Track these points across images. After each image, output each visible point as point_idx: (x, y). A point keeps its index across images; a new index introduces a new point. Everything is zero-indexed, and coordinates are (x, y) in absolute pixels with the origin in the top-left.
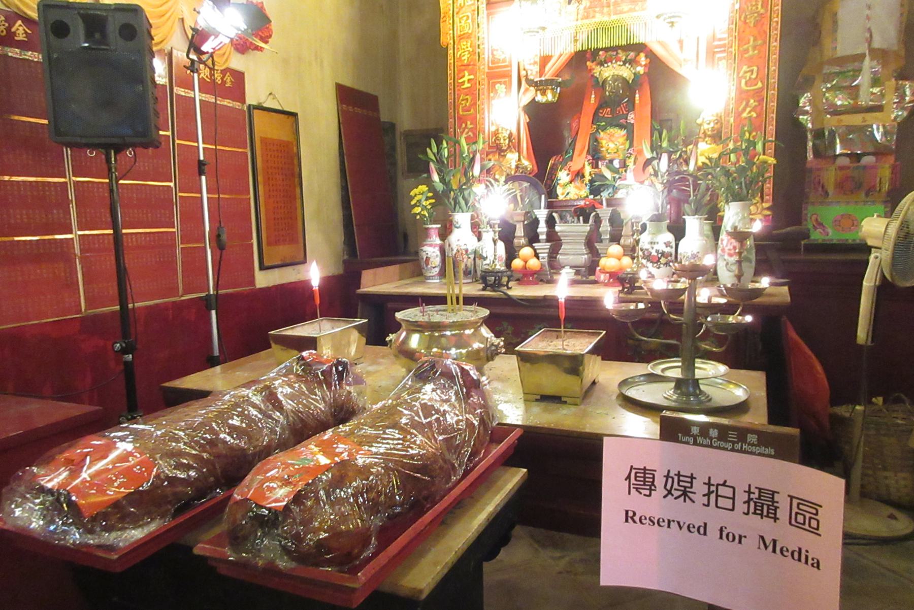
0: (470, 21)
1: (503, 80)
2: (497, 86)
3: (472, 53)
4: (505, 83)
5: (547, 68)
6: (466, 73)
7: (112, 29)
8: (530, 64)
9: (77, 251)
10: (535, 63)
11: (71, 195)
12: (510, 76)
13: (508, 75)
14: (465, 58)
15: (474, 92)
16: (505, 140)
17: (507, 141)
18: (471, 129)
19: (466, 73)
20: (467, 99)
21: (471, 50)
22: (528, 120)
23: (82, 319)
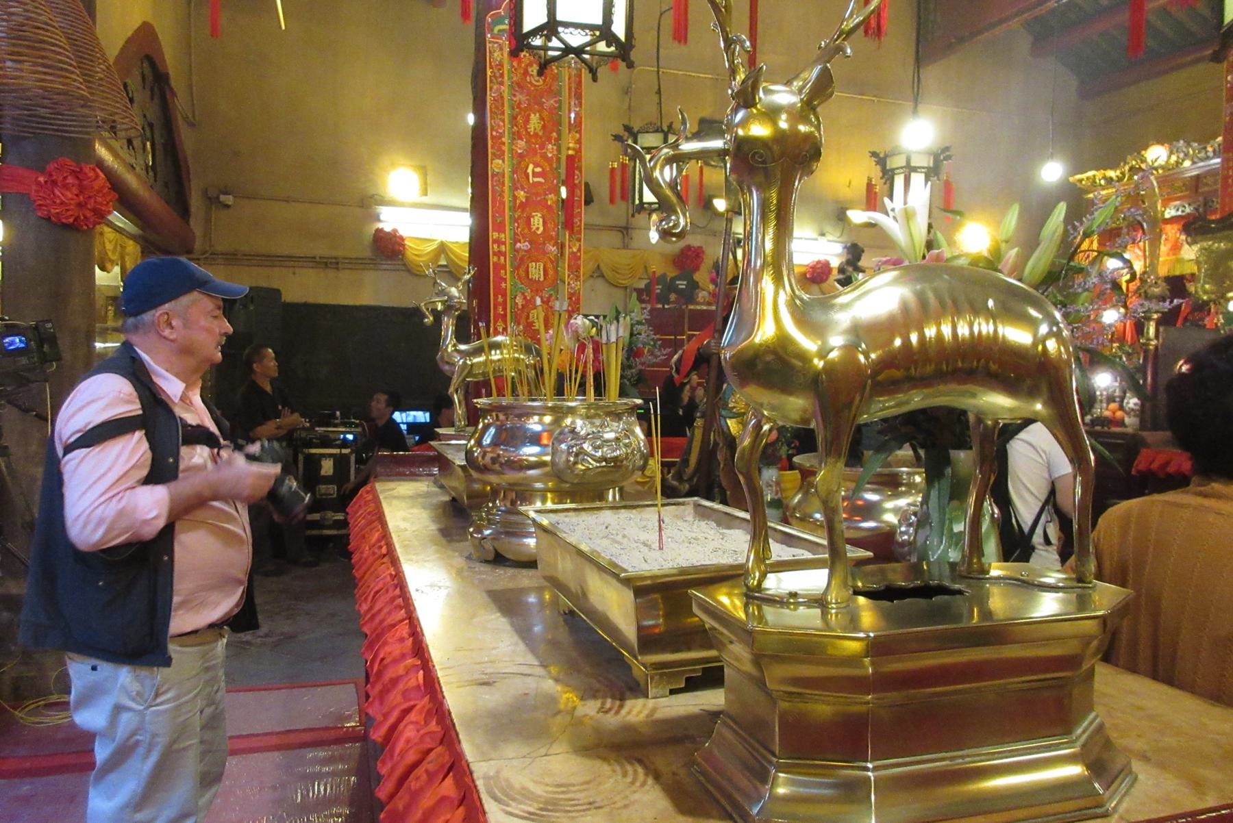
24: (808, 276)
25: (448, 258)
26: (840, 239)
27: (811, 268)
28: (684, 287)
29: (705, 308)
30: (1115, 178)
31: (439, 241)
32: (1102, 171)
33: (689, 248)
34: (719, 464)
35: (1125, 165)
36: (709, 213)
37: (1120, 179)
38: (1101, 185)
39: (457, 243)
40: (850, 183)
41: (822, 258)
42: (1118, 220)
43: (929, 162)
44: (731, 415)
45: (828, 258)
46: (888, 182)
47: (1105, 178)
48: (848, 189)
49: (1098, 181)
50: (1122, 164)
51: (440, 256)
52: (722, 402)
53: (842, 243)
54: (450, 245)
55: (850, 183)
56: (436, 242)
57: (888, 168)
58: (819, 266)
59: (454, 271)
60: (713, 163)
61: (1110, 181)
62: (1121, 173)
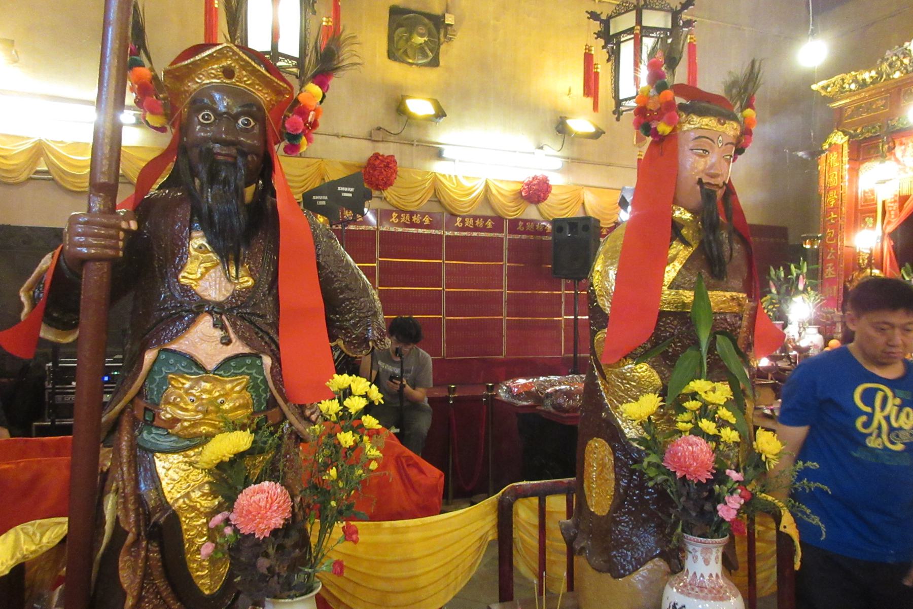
0: (836, 177)
1: (871, 214)
2: (867, 219)
3: (837, 200)
4: (873, 217)
5: (905, 205)
6: (832, 213)
7: (580, 226)
8: (891, 202)
9: (563, 326)
10: (895, 201)
11: (563, 300)
12: (876, 211)
13: (875, 211)
14: (832, 203)
15: (836, 227)
16: (863, 260)
17: (866, 261)
18: (833, 254)
19: (832, 213)
20: (832, 233)
21: (836, 197)
22: (892, 244)
23: (563, 359)
24: (523, 194)
25: (49, 162)
26: (559, 154)
27: (527, 184)
28: (350, 195)
29: (400, 230)
30: (869, 80)
31: (37, 138)
32: (853, 73)
33: (376, 156)
34: (124, 595)
35: (882, 62)
36: (405, 118)
37: (874, 81)
38: (851, 91)
39: (62, 142)
40: (570, 91)
41: (540, 174)
42: (874, 128)
43: (666, 22)
44: (166, 443)
45: (546, 174)
46: (613, 58)
47: (855, 81)
48: (567, 98)
49: (846, 86)
50: (878, 62)
51: (39, 158)
52: (142, 404)
53: (564, 158)
54: (52, 145)
55: (570, 91)
56: (32, 141)
57: (612, 33)
58: (535, 182)
59: (57, 178)
60: (410, 61)
61: (863, 85)
62: (877, 73)
